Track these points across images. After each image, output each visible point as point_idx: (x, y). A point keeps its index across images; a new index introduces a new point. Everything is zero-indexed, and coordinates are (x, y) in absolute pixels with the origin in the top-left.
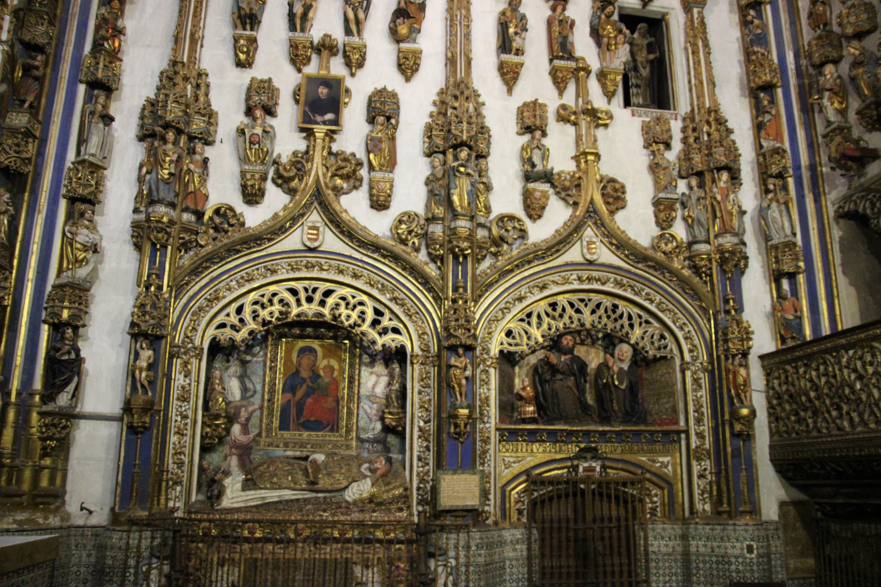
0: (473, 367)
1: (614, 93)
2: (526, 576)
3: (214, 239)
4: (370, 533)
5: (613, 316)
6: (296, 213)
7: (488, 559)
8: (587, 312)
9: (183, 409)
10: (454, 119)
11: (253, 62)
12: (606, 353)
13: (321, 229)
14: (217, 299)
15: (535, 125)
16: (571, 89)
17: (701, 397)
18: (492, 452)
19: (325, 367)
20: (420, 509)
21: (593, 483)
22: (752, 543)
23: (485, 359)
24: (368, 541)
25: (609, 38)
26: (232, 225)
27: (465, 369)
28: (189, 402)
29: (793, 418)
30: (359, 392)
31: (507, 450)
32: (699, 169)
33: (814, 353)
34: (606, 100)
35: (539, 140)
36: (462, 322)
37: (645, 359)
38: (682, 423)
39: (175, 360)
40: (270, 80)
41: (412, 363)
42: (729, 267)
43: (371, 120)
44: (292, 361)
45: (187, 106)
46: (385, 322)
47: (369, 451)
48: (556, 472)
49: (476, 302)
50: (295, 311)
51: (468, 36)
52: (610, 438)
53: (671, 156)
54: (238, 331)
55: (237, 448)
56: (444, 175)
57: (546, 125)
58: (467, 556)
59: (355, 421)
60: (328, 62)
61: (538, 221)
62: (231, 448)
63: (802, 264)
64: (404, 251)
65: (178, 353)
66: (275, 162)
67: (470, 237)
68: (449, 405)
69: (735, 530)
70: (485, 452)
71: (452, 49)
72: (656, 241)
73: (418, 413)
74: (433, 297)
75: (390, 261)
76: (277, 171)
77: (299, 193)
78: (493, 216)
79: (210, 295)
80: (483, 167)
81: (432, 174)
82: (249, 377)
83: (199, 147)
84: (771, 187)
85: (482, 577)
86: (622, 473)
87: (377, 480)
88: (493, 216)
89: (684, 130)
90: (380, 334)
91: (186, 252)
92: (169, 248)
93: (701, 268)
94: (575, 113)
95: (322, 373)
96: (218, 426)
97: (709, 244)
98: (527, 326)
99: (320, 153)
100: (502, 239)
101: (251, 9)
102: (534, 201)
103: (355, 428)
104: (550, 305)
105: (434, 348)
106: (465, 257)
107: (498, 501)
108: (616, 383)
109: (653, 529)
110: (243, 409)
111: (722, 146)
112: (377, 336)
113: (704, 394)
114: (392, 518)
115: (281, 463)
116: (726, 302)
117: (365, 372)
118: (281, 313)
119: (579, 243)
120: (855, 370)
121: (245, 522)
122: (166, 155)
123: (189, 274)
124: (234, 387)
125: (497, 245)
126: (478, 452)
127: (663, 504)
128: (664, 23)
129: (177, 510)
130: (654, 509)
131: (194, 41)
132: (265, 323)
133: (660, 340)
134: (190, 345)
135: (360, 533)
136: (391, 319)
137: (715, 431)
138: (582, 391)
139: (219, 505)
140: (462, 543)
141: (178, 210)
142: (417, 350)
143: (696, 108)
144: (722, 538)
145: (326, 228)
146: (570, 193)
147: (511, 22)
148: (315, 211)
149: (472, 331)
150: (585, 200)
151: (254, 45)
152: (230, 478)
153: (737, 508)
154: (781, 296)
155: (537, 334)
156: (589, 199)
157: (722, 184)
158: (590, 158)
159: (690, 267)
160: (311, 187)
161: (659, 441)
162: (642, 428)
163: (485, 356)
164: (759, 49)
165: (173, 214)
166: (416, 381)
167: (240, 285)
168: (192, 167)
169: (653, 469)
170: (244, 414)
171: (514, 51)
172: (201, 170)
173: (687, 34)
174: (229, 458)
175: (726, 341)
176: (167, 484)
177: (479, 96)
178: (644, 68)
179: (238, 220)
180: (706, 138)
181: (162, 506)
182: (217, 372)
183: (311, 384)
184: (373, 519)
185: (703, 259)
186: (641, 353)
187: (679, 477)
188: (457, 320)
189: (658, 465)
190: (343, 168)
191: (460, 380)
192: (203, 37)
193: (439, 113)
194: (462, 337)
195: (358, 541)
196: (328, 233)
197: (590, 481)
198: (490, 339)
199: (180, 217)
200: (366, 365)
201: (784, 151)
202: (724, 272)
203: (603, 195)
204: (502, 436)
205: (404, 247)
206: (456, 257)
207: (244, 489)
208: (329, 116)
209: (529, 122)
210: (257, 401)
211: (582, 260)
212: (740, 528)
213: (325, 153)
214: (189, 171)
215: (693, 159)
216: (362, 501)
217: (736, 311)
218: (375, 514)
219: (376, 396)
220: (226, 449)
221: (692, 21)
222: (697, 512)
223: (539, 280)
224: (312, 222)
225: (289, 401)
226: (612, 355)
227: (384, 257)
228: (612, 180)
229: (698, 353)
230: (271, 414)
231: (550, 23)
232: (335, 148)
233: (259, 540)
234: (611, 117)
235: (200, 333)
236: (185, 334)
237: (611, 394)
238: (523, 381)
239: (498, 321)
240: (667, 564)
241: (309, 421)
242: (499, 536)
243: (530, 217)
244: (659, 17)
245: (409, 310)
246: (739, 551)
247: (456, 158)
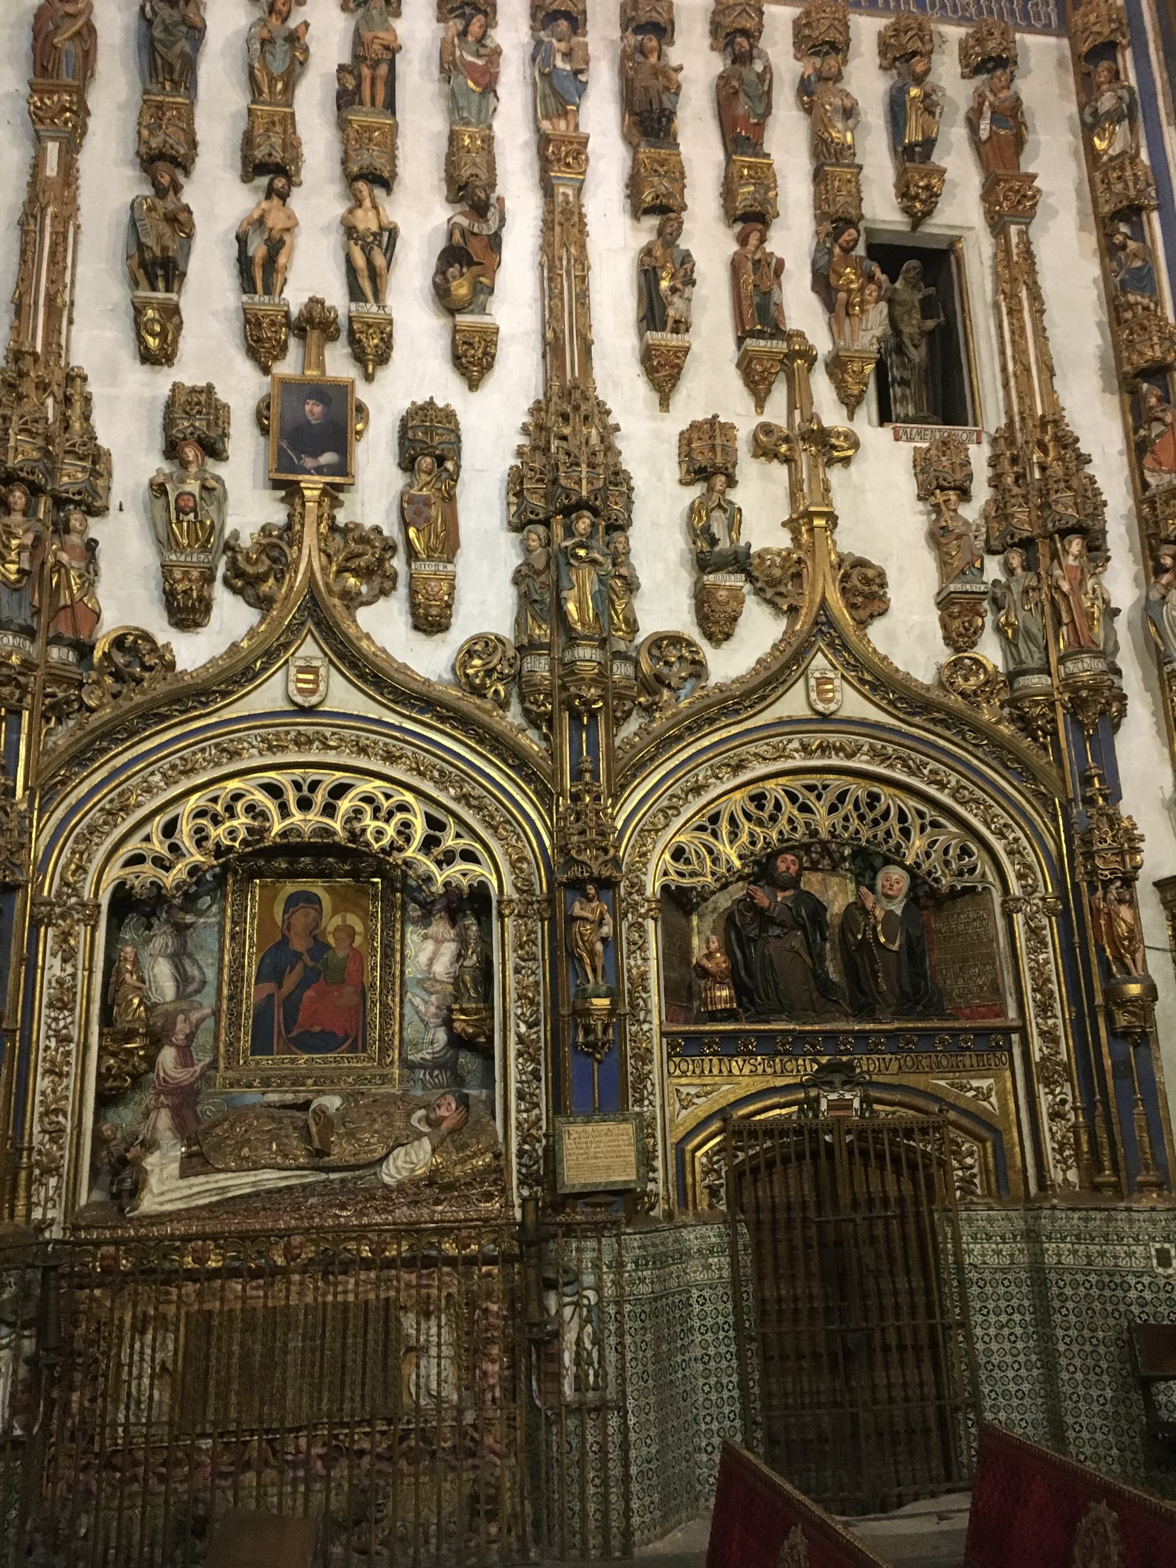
0: (614, 919)
1: (860, 399)
2: (731, 1319)
3: (115, 696)
4: (431, 1244)
5: (871, 816)
6: (273, 642)
7: (657, 1287)
8: (820, 808)
9: (62, 1023)
10: (562, 457)
11: (174, 354)
12: (858, 884)
13: (322, 671)
14: (126, 809)
15: (714, 465)
16: (779, 395)
17: (1047, 962)
18: (655, 1077)
19: (337, 929)
20: (526, 1192)
21: (849, 1132)
22: (1167, 1246)
23: (637, 903)
24: (429, 1262)
25: (849, 291)
26: (150, 669)
27: (601, 923)
28: (72, 1010)
30: (402, 972)
31: (684, 1074)
32: (1026, 534)
34: (845, 412)
35: (723, 493)
36: (592, 835)
37: (933, 894)
38: (1012, 1013)
39: (43, 929)
40: (210, 388)
41: (501, 916)
42: (1089, 715)
43: (408, 464)
44: (274, 922)
45: (49, 439)
46: (449, 841)
47: (424, 1088)
48: (777, 1111)
49: (616, 797)
50: (277, 826)
51: (583, 298)
52: (876, 1045)
53: (971, 512)
54: (167, 869)
55: (169, 1093)
56: (548, 563)
57: (735, 465)
58: (616, 1284)
59: (397, 1028)
60: (321, 353)
61: (725, 645)
62: (158, 1094)
64: (478, 707)
65: (49, 916)
66: (228, 547)
67: (602, 678)
68: (573, 991)
69: (1131, 1221)
70: (643, 1078)
71: (554, 324)
72: (947, 672)
73: (514, 1009)
74: (536, 792)
75: (454, 728)
76: (233, 564)
77: (277, 606)
78: (640, 638)
79: (111, 801)
80: (620, 547)
81: (526, 563)
82: (190, 956)
83: (76, 520)
84: (1168, 561)
85: (648, 1324)
86: (902, 1111)
88: (640, 638)
89: (994, 462)
90: (439, 863)
91: (59, 721)
92: (26, 714)
93: (1036, 719)
94: (787, 440)
95: (331, 940)
96: (131, 1052)
97: (1050, 675)
98: (711, 839)
99: (314, 529)
100: (659, 679)
101: (164, 249)
102: (717, 608)
103: (396, 1042)
104: (752, 798)
105: (541, 886)
106: (593, 715)
107: (672, 1171)
108: (882, 940)
109: (969, 1220)
110: (181, 1017)
111: (1069, 488)
112: (434, 868)
113: (1050, 955)
114: (473, 1215)
115: (257, 1118)
116: (1087, 781)
117: (413, 936)
118: (250, 830)
119: (802, 681)
121: (187, 1239)
122: (11, 535)
123: (68, 764)
124: (162, 975)
125: (652, 692)
126: (630, 1078)
127: (985, 1170)
128: (952, 258)
129: (51, 1225)
130: (968, 1181)
131: (54, 312)
132: (219, 851)
133: (960, 858)
134: (73, 900)
135: (411, 1246)
136: (458, 836)
137: (1078, 1026)
138: (819, 958)
139: (133, 1209)
140: (606, 1259)
141: (40, 641)
142: (508, 889)
143: (1017, 418)
144: (1106, 1237)
145: (332, 670)
146: (782, 589)
147: (663, 268)
148: (309, 638)
149: (612, 852)
150: (812, 601)
151: (175, 320)
152: (157, 1153)
153: (1131, 1177)
155: (730, 853)
156: (818, 599)
157: (1071, 561)
158: (818, 522)
159: (1012, 720)
160: (299, 591)
161: (968, 1049)
162: (936, 1024)
163: (636, 897)
164: (1139, 298)
165: (31, 649)
166: (509, 949)
167: (169, 782)
168: (64, 557)
169: (961, 1103)
170: (182, 1027)
171: (670, 323)
172: (82, 564)
174: (153, 1115)
175: (1089, 856)
176: (30, 1174)
177: (608, 413)
178: (916, 346)
179: (162, 657)
180: (1037, 475)
181: (19, 1219)
182: (129, 949)
183: (310, 963)
184: (437, 1217)
185: (1037, 703)
186: (925, 882)
187: (1013, 1117)
188: (582, 832)
189: (971, 1094)
190: (359, 555)
191: (592, 944)
192: (72, 303)
193: (535, 448)
194: (591, 863)
195: (409, 1263)
196: (336, 678)
197: (844, 1128)
198: (645, 864)
199: (46, 654)
200: (415, 923)
202: (1080, 726)
203: (844, 591)
204: (672, 1046)
205: (478, 701)
206: (575, 717)
207: (183, 1175)
208: (328, 458)
209: (701, 460)
210: (207, 1000)
211: (808, 713)
212: (1141, 1216)
213: (323, 529)
214: (59, 563)
215: (1013, 516)
216: (415, 1182)
217: (1105, 798)
218: (440, 1208)
219: (437, 981)
220: (148, 1098)
221: (1008, 251)
222: (1053, 1186)
223: (731, 753)
224: (305, 658)
226: (872, 889)
227: (442, 719)
228: (861, 563)
229: (1035, 880)
230: (235, 1023)
231: (735, 267)
232: (341, 518)
233: (216, 1273)
234: (856, 445)
235: (92, 876)
236: (62, 878)
237: (872, 960)
238: (708, 941)
239: (657, 831)
240: (1001, 1290)
241: (308, 1032)
242: (676, 1241)
243: (710, 637)
244: (944, 247)
245: (493, 818)
246: (1143, 1263)
247: (569, 532)
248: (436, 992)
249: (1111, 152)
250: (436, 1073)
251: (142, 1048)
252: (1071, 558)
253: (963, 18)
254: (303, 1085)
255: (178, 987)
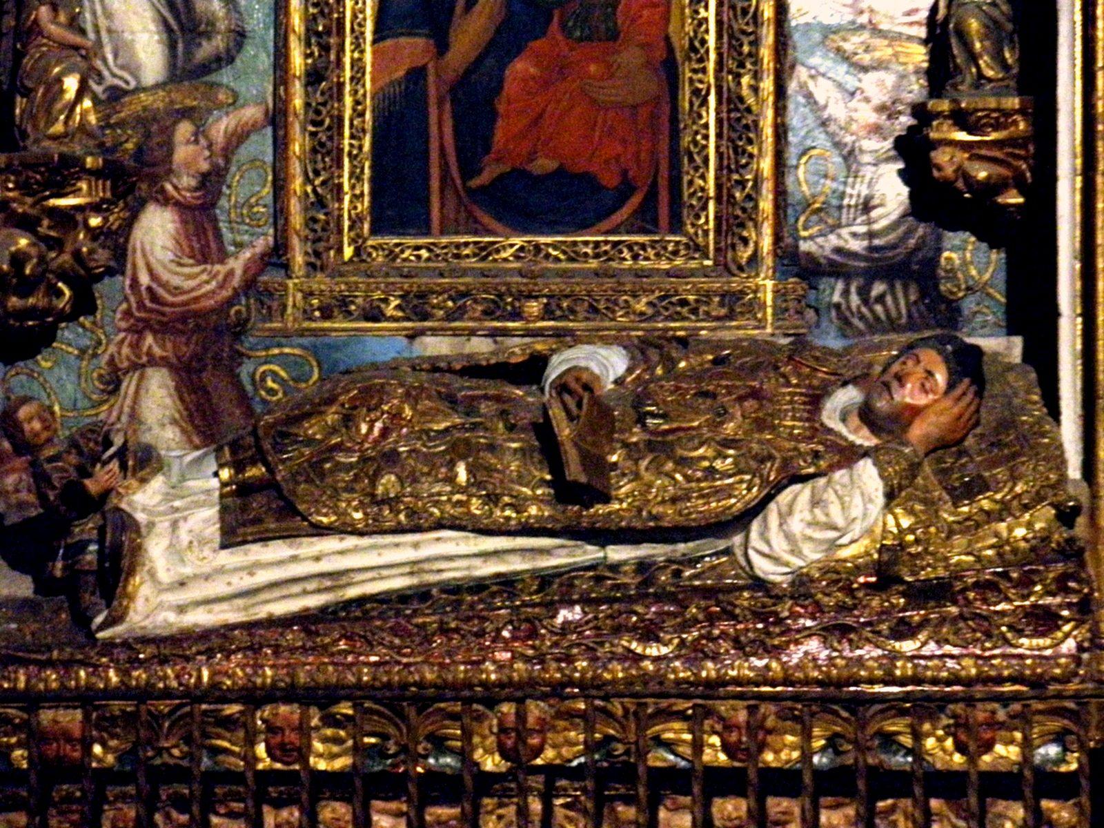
4: (889, 741)
47: (845, 323)
55: (163, 328)
59: (766, 165)
62: (138, 330)
87: (914, 469)
96: (66, 219)
103: (766, 204)
110: (184, 129)
115: (411, 396)
121: (253, 697)
135: (832, 743)
152: (157, 483)
174: (129, 385)
184: (902, 668)
207: (231, 537)
218: (908, 646)
219: (876, 31)
225: (417, 75)
233: (333, 785)
241: (519, 174)
248: (879, 66)
250: (878, 288)
251: (95, 208)
254: (516, 315)
255: (172, 46)
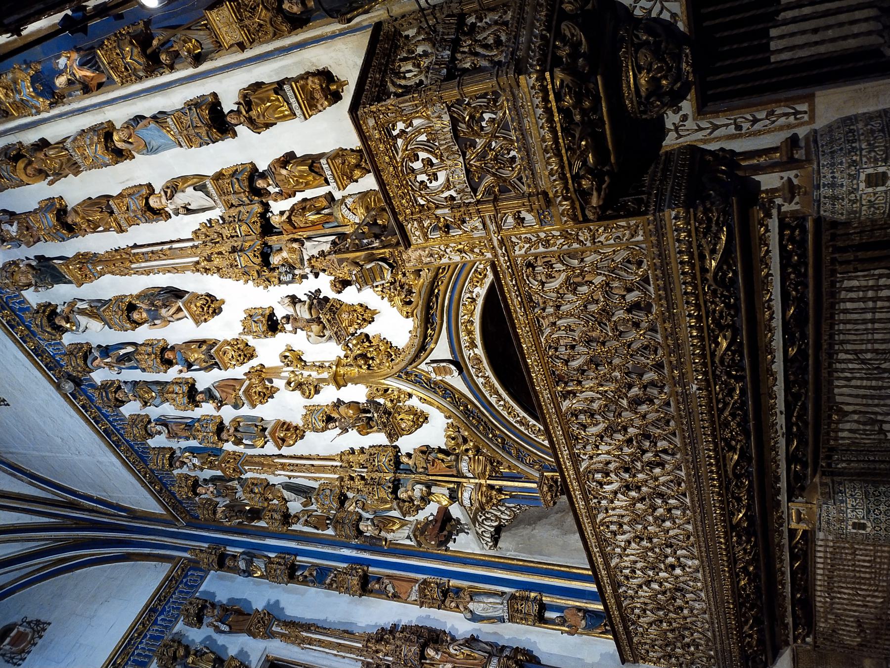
29: (692, 649)
33: (621, 615)
63: (533, 595)
120: (640, 586)
154: (563, 621)
173: (293, 643)
201: (425, 580)
221: (282, 635)
249: (263, 570)
252: (436, 656)
253: (176, 619)
